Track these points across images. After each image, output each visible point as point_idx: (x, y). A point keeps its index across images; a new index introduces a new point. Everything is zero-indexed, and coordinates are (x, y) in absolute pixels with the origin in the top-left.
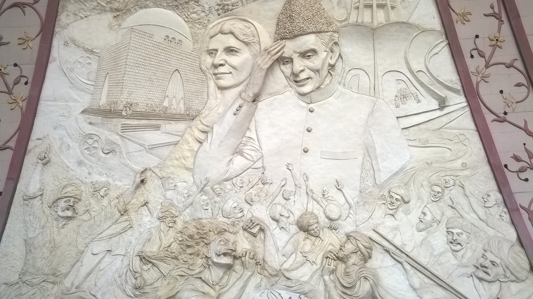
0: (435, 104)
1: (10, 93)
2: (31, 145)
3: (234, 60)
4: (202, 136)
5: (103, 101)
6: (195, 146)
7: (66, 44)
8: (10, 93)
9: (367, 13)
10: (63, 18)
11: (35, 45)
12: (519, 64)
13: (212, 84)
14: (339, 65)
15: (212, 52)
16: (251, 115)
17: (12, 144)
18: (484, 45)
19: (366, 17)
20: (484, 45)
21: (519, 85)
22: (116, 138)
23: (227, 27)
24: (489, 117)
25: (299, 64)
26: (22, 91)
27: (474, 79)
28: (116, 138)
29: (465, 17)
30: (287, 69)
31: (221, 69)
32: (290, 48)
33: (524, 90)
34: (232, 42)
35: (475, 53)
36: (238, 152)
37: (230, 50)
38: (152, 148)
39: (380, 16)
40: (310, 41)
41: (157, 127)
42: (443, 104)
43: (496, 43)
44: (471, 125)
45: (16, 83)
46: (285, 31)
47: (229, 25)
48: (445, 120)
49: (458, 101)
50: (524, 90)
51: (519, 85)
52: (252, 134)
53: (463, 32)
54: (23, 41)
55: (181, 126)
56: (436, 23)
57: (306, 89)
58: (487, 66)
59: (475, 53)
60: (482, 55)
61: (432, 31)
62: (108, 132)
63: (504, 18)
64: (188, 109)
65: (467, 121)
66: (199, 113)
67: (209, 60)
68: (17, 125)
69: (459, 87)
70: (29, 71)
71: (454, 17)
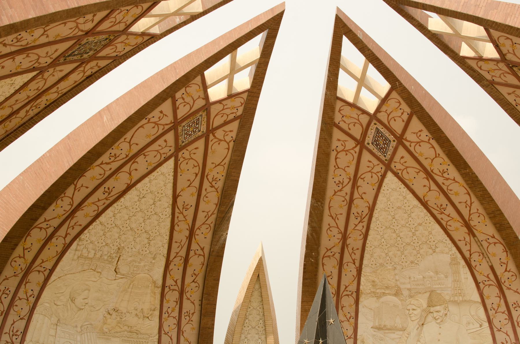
0: (479, 326)
1: (349, 321)
2: (358, 337)
3: (415, 312)
4: (407, 336)
5: (377, 324)
6: (406, 338)
7: (363, 307)
8: (349, 321)
9: (456, 297)
10: (361, 299)
11: (354, 307)
12: (506, 312)
13: (409, 319)
14: (448, 313)
15: (409, 310)
16: (421, 330)
17: (353, 336)
18: (495, 306)
19: (456, 299)
20: (495, 306)
21: (506, 319)
22: (382, 336)
23: (412, 303)
24: (495, 329)
25: (435, 314)
26: (352, 321)
27: (491, 318)
28: (382, 336)
29: (488, 297)
30: (432, 314)
31: (411, 315)
32: (432, 309)
33: (507, 321)
34: (414, 307)
35: (492, 309)
36: (419, 341)
37: (414, 310)
38: (393, 339)
39: (461, 298)
40: (438, 308)
41: (394, 333)
42: (481, 326)
43: (499, 306)
44: (490, 332)
45: (350, 318)
46: (430, 304)
47: (413, 301)
48: (481, 331)
49: (486, 324)
50: (507, 321)
51: (506, 319)
52: (422, 335)
53: (488, 302)
54: (350, 306)
55: (401, 333)
56: (479, 300)
57: (438, 321)
58: (496, 313)
59: (492, 309)
60: (494, 309)
61: (478, 302)
62: (380, 334)
63: (502, 297)
64: (403, 327)
65: (488, 331)
66: (406, 328)
67: (408, 312)
68: (353, 331)
69: (486, 319)
70: (353, 314)
71: (485, 297)
